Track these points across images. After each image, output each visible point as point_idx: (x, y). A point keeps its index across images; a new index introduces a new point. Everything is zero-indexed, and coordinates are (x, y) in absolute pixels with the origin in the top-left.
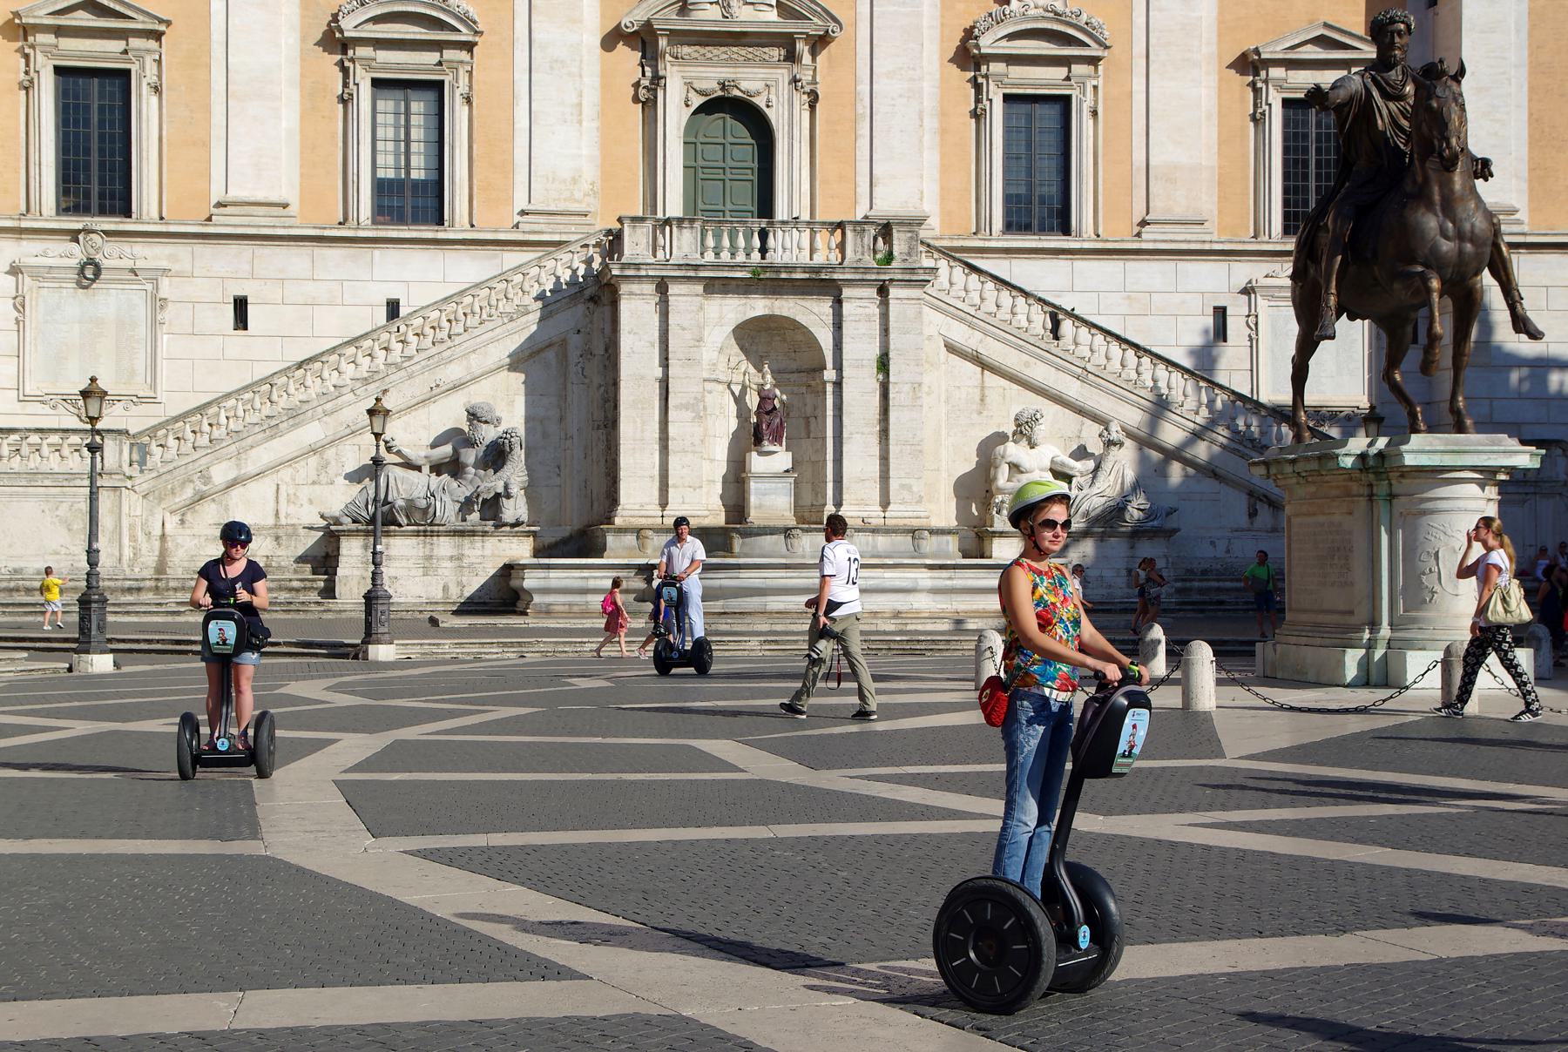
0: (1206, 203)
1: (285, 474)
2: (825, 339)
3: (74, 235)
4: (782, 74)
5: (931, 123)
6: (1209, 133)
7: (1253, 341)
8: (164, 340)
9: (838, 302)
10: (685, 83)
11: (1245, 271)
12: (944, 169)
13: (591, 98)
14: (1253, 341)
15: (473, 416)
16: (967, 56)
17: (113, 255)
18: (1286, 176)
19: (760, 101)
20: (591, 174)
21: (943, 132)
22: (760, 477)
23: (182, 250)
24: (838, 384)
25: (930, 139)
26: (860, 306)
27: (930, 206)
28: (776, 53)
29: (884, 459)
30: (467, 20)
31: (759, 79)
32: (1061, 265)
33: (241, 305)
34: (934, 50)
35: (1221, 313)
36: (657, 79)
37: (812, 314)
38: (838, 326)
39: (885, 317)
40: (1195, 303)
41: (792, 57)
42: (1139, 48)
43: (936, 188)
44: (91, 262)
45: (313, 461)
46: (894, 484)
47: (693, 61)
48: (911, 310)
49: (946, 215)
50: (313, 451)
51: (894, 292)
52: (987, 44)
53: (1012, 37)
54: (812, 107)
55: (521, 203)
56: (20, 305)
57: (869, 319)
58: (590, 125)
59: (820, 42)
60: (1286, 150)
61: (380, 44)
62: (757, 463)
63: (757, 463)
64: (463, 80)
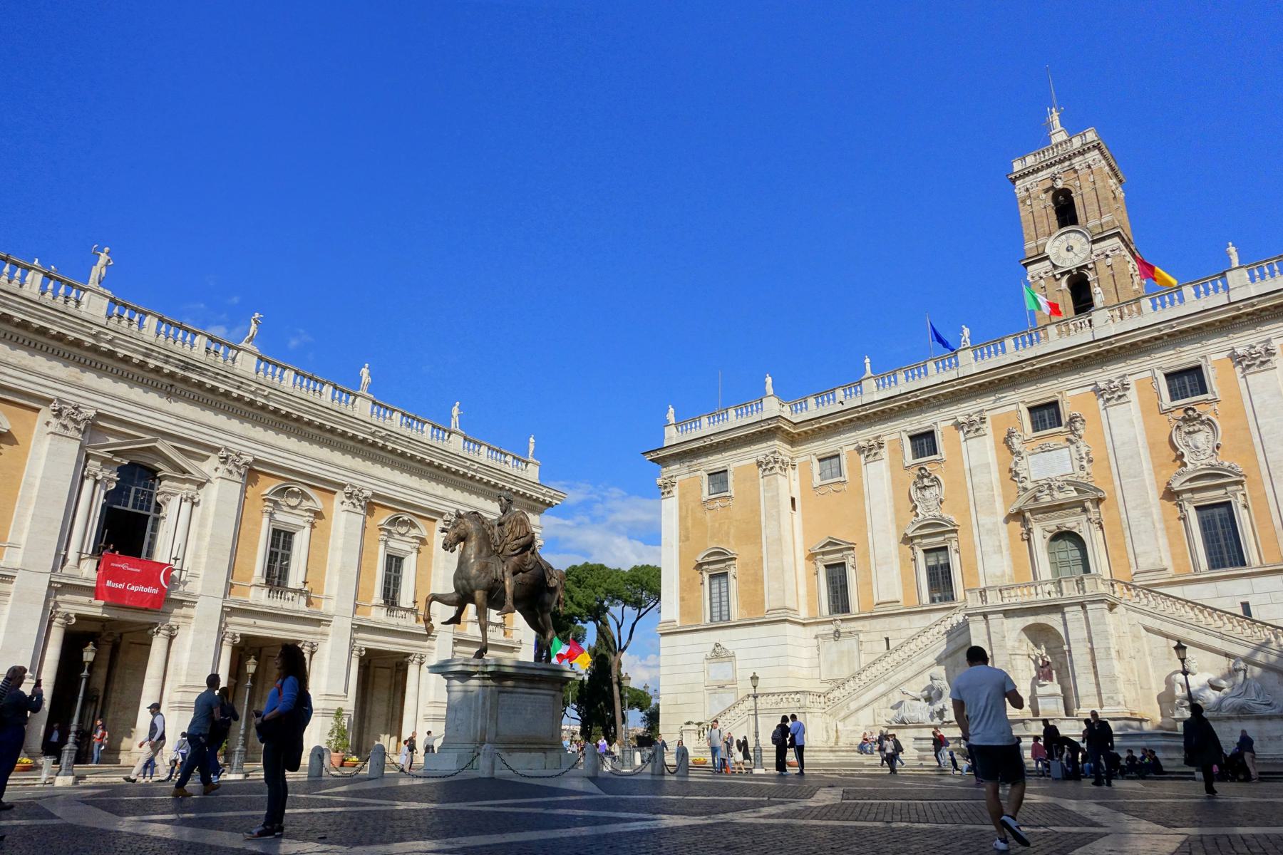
1: (876, 705)
2: (1061, 630)
3: (831, 622)
4: (1084, 517)
9: (1063, 614)
10: (1040, 532)
12: (1171, 545)
13: (1005, 542)
15: (932, 678)
16: (1170, 495)
17: (844, 627)
19: (1076, 530)
21: (1167, 528)
22: (1042, 696)
24: (1070, 651)
26: (1073, 614)
27: (1167, 562)
28: (1079, 510)
29: (1098, 685)
30: (950, 522)
31: (1072, 522)
32: (1245, 581)
33: (887, 639)
34: (1154, 495)
36: (1029, 531)
37: (1054, 620)
38: (1065, 625)
39: (1087, 618)
41: (1085, 510)
42: (1264, 472)
43: (1169, 554)
44: (837, 631)
45: (885, 699)
46: (1104, 697)
47: (1044, 520)
48: (1098, 614)
50: (884, 695)
51: (1089, 607)
52: (1176, 486)
54: (1101, 528)
57: (1078, 620)
59: (1099, 501)
61: (922, 537)
62: (1040, 691)
63: (1040, 691)
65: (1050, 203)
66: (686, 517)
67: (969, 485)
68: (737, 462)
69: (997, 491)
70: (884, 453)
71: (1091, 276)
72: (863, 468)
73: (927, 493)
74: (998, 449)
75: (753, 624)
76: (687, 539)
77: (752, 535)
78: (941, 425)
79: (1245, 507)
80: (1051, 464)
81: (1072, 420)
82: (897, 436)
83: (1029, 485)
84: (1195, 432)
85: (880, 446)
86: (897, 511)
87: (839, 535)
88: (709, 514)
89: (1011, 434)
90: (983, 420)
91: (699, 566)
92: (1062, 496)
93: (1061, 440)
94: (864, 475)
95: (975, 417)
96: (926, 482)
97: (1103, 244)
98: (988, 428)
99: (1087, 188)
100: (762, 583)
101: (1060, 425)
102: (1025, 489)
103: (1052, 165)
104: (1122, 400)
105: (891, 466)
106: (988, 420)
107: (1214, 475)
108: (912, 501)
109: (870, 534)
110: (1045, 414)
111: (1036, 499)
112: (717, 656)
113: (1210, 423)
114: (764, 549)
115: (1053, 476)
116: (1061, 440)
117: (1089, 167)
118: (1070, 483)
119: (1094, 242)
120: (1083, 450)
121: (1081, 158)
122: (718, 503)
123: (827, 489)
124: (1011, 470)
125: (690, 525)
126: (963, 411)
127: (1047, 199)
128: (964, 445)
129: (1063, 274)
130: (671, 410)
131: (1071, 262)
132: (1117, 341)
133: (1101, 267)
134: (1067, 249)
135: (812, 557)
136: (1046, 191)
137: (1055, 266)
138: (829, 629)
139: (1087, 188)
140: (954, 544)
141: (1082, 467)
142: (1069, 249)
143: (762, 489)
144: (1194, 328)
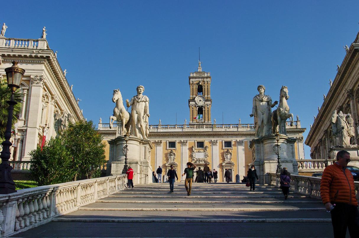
65: (197, 87)
70: (162, 144)
73: (172, 157)
78: (177, 141)
79: (234, 170)
80: (199, 155)
81: (206, 147)
83: (195, 159)
84: (228, 155)
85: (161, 143)
86: (163, 159)
89: (193, 147)
90: (187, 142)
92: (201, 162)
95: (185, 141)
97: (208, 102)
98: (188, 144)
99: (206, 87)
103: (200, 78)
104: (216, 145)
105: (163, 148)
106: (188, 142)
110: (201, 145)
113: (231, 154)
115: (200, 158)
117: (207, 82)
119: (206, 101)
120: (207, 154)
121: (206, 79)
126: (182, 139)
129: (198, 106)
131: (201, 104)
132: (220, 133)
133: (206, 107)
134: (199, 101)
136: (197, 84)
137: (196, 103)
139: (206, 87)
141: (206, 157)
142: (200, 101)
144: (232, 134)
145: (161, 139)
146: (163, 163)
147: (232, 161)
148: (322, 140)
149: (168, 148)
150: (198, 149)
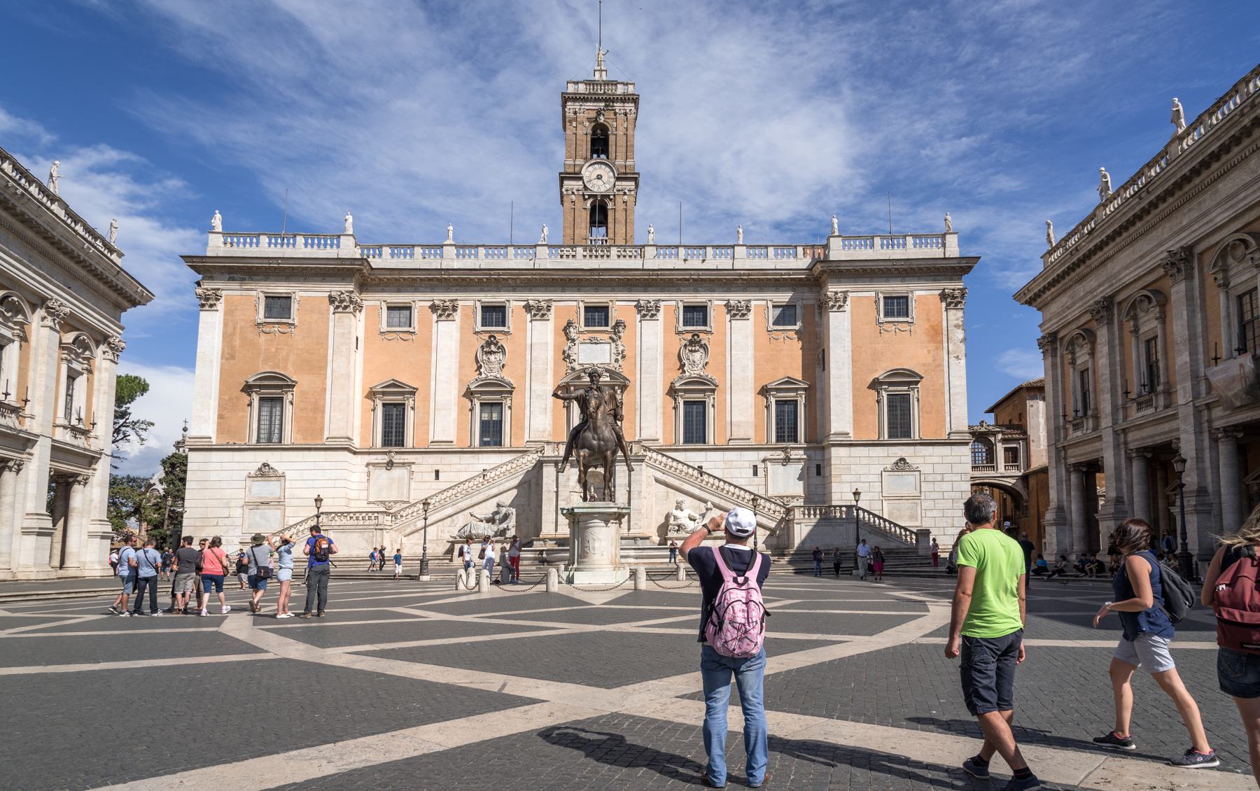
0: (751, 433)
5: (660, 410)
6: (752, 411)
7: (766, 476)
8: (413, 484)
11: (763, 454)
12: (664, 424)
14: (766, 476)
17: (397, 459)
18: (777, 424)
20: (549, 429)
21: (664, 413)
23: (419, 457)
25: (660, 415)
27: (660, 436)
30: (509, 384)
35: (755, 467)
40: (747, 464)
49: (665, 439)
52: (677, 386)
53: (685, 384)
55: (527, 438)
56: (369, 475)
58: (549, 415)
60: (777, 416)
64: (509, 402)
66: (233, 334)
67: (528, 357)
68: (305, 295)
69: (551, 366)
70: (457, 316)
71: (610, 206)
72: (435, 325)
73: (492, 357)
74: (556, 333)
75: (309, 449)
76: (233, 357)
77: (318, 366)
78: (513, 304)
82: (471, 303)
85: (455, 309)
86: (461, 367)
87: (403, 378)
88: (263, 336)
89: (569, 324)
91: (248, 389)
93: (606, 337)
94: (434, 330)
96: (493, 348)
98: (551, 315)
100: (324, 412)
101: (607, 325)
102: (573, 369)
105: (462, 328)
106: (553, 309)
107: (701, 381)
108: (477, 361)
109: (433, 383)
110: (597, 315)
111: (579, 377)
112: (262, 476)
113: (705, 347)
114: (329, 381)
115: (595, 362)
116: (606, 337)
118: (607, 371)
122: (276, 328)
123: (394, 335)
124: (564, 352)
125: (237, 343)
127: (588, 127)
128: (529, 325)
130: (218, 216)
135: (372, 395)
138: (385, 459)
140: (509, 402)
141: (617, 361)
143: (331, 324)
145: (453, 296)
146: (460, 381)
147: (709, 373)
148: (1192, 254)
149: (479, 328)
150: (588, 332)
